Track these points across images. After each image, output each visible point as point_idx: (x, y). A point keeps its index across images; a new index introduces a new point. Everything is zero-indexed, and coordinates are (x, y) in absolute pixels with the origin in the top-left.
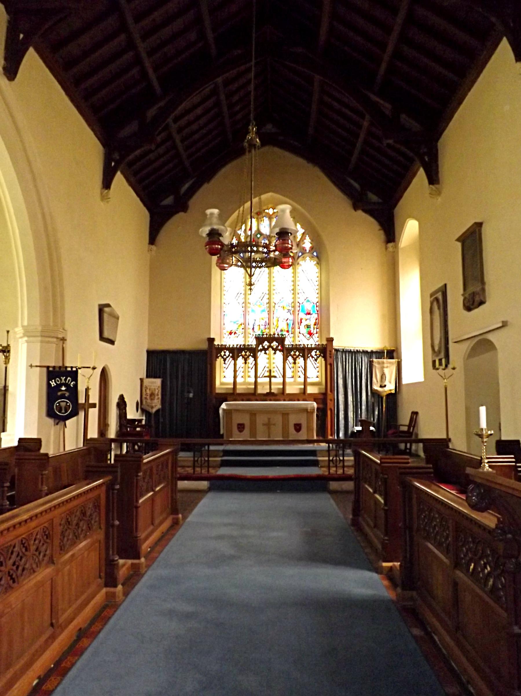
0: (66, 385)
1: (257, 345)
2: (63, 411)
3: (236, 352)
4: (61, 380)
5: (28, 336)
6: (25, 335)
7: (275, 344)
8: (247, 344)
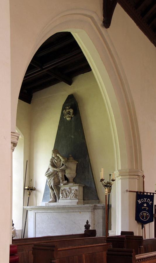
0: (147, 203)
2: (145, 218)
4: (144, 200)
5: (121, 176)
6: (120, 175)
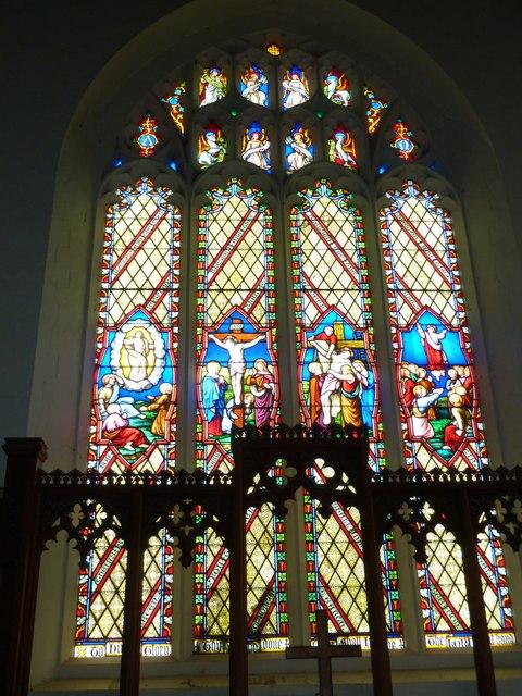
1: (241, 475)
3: (141, 508)
7: (323, 471)
8: (190, 470)
